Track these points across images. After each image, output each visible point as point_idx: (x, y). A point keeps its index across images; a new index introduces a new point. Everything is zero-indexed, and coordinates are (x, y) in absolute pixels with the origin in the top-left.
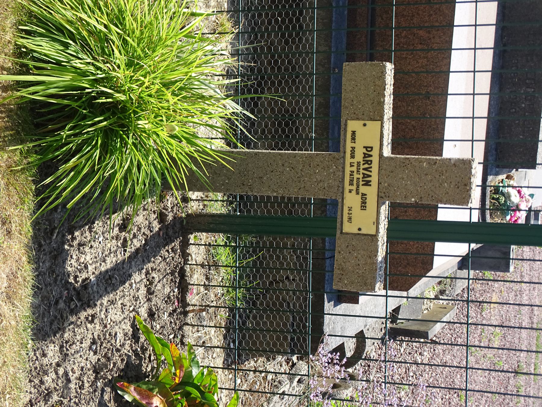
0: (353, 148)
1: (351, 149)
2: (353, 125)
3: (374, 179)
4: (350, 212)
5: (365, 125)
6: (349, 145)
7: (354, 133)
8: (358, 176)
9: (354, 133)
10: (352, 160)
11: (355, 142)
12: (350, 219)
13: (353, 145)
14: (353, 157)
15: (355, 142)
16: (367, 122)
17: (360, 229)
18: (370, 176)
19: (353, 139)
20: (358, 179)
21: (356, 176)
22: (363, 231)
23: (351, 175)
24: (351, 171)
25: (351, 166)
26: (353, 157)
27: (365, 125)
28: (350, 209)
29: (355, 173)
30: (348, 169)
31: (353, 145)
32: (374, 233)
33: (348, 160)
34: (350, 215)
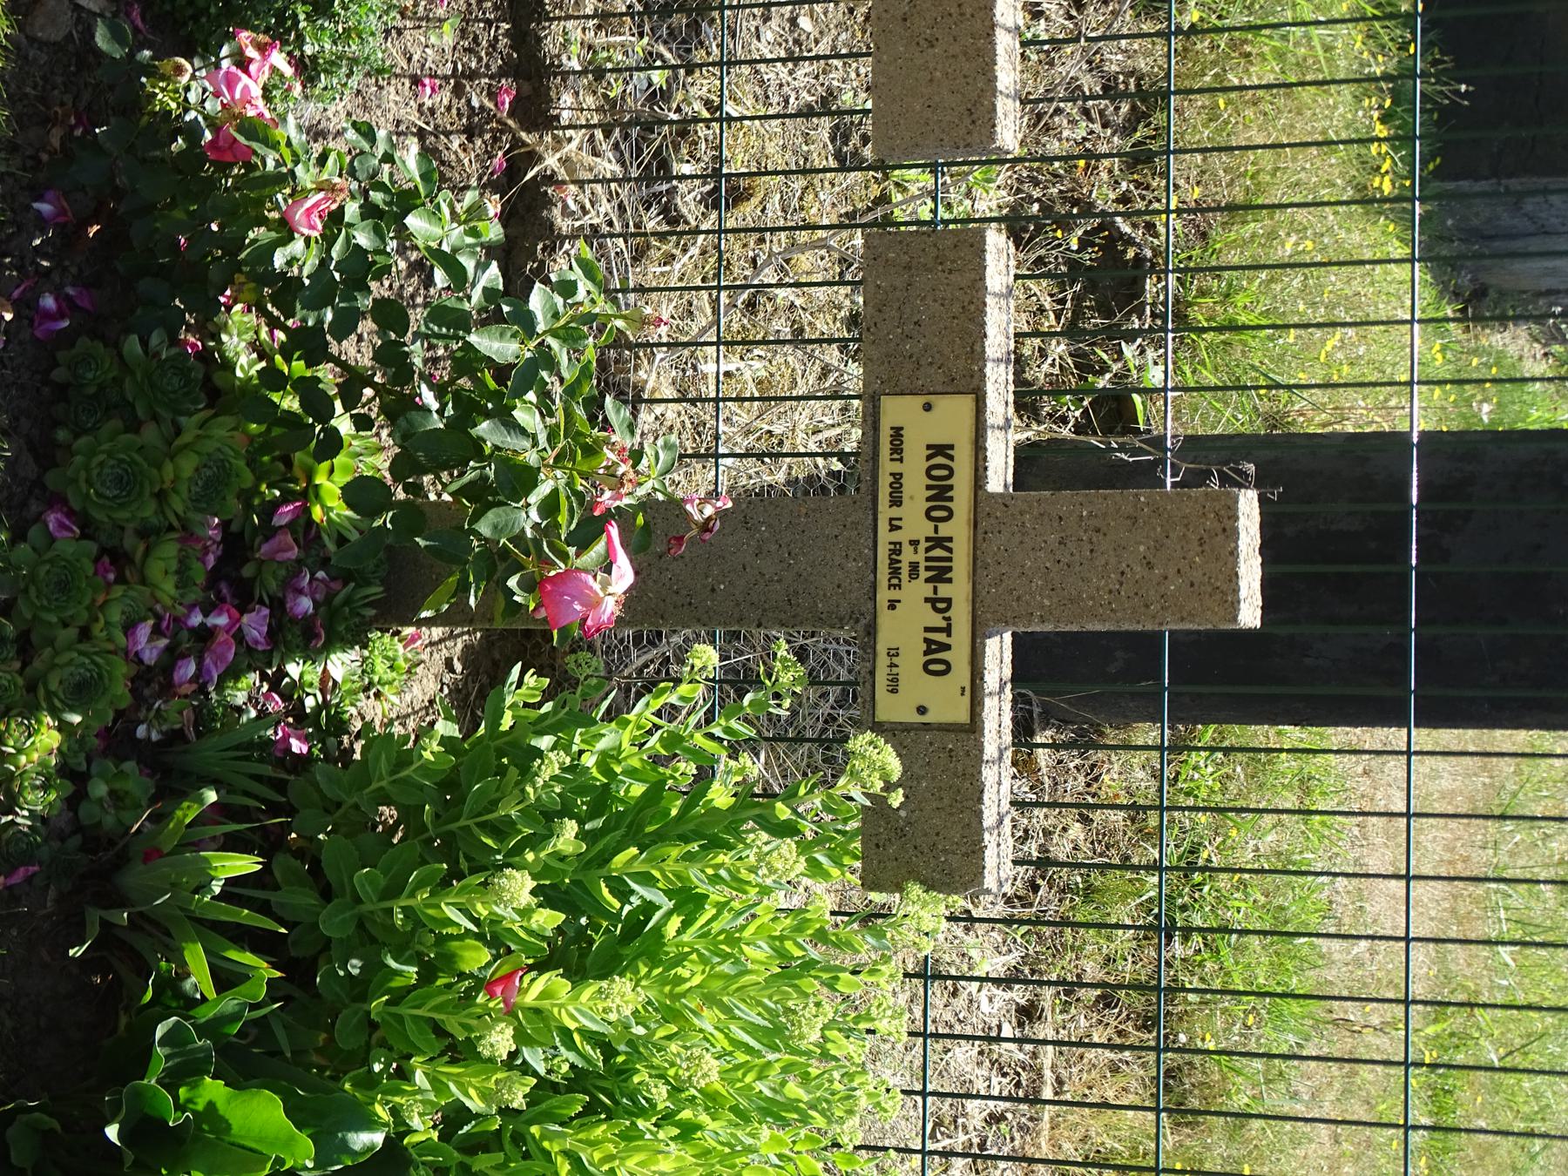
0: (897, 477)
1: (891, 479)
4: (895, 660)
6: (887, 467)
7: (897, 433)
8: (914, 558)
11: (901, 460)
13: (896, 467)
14: (896, 502)
15: (901, 460)
17: (922, 710)
18: (947, 647)
19: (897, 450)
21: (908, 555)
25: (894, 528)
27: (928, 407)
28: (893, 653)
31: (896, 467)
32: (963, 716)
33: (885, 511)
34: (895, 670)
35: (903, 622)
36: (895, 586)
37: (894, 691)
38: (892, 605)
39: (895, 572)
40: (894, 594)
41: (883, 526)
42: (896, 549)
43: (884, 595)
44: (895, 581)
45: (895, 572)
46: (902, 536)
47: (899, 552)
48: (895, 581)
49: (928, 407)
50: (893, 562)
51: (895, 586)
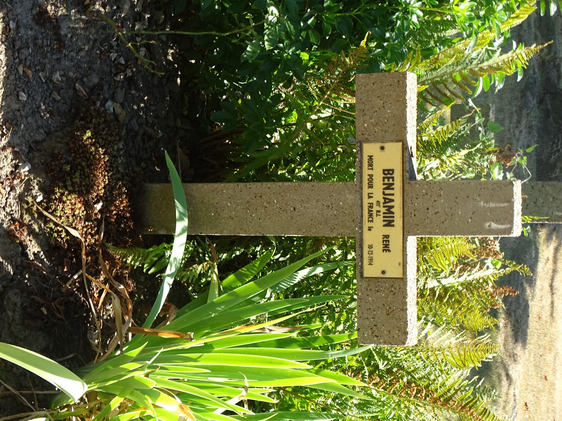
0: (371, 176)
2: (369, 149)
5: (382, 148)
6: (366, 172)
7: (371, 158)
8: (378, 208)
9: (371, 158)
10: (370, 190)
11: (372, 169)
12: (371, 259)
13: (370, 172)
14: (371, 186)
15: (372, 169)
16: (387, 145)
17: (383, 272)
19: (371, 165)
20: (379, 211)
22: (387, 275)
24: (370, 204)
26: (371, 186)
27: (382, 148)
28: (370, 247)
30: (366, 201)
31: (370, 172)
32: (400, 276)
33: (366, 190)
34: (371, 256)
36: (371, 221)
37: (370, 264)
38: (370, 229)
39: (371, 215)
40: (370, 224)
42: (371, 206)
43: (366, 225)
44: (371, 219)
45: (371, 215)
48: (371, 219)
50: (369, 211)
51: (371, 221)
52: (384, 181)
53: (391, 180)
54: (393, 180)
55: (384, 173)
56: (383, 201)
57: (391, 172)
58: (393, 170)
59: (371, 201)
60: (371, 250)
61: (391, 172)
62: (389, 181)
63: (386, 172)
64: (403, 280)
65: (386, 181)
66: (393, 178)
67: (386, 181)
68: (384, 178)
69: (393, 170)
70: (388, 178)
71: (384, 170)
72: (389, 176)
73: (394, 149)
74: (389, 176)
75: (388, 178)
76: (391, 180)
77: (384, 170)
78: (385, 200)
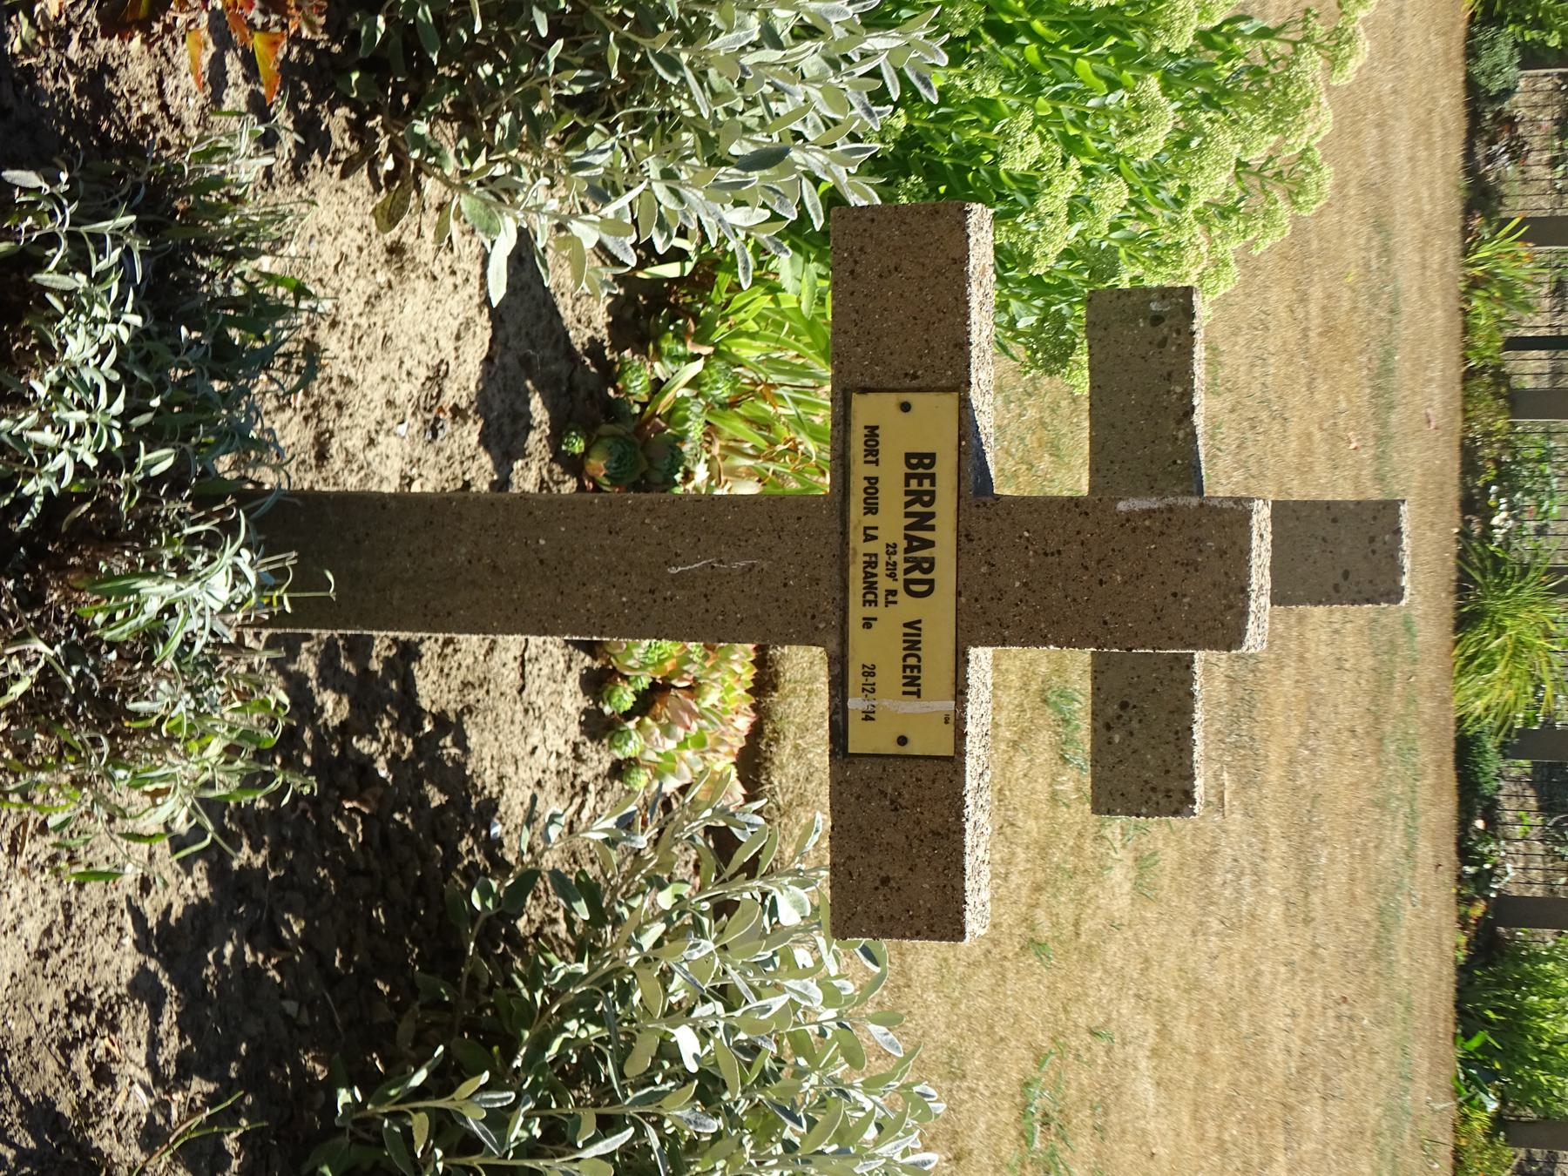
0: (872, 481)
1: (866, 484)
3: (945, 575)
6: (860, 470)
7: (872, 432)
9: (872, 432)
10: (870, 520)
11: (876, 463)
13: (871, 471)
14: (871, 509)
15: (876, 463)
17: (902, 741)
19: (872, 451)
22: (914, 748)
23: (868, 564)
24: (870, 555)
26: (871, 509)
27: (906, 407)
29: (883, 559)
31: (871, 471)
32: (948, 751)
35: (877, 646)
36: (870, 602)
38: (868, 623)
39: (871, 587)
40: (870, 611)
41: (856, 538)
42: (871, 563)
43: (857, 611)
44: (870, 597)
45: (871, 587)
46: (877, 547)
47: (874, 564)
48: (870, 597)
49: (906, 407)
50: (868, 575)
51: (870, 602)
52: (907, 484)
53: (927, 482)
54: (933, 484)
55: (908, 465)
56: (903, 544)
57: (927, 461)
58: (932, 456)
59: (871, 547)
60: (871, 680)
61: (927, 461)
62: (920, 484)
63: (914, 461)
64: (954, 763)
65: (914, 484)
66: (932, 477)
67: (914, 484)
68: (908, 477)
69: (932, 456)
70: (921, 478)
71: (908, 456)
72: (920, 471)
73: (935, 409)
74: (920, 471)
75: (921, 478)
76: (926, 484)
77: (908, 456)
78: (910, 544)
